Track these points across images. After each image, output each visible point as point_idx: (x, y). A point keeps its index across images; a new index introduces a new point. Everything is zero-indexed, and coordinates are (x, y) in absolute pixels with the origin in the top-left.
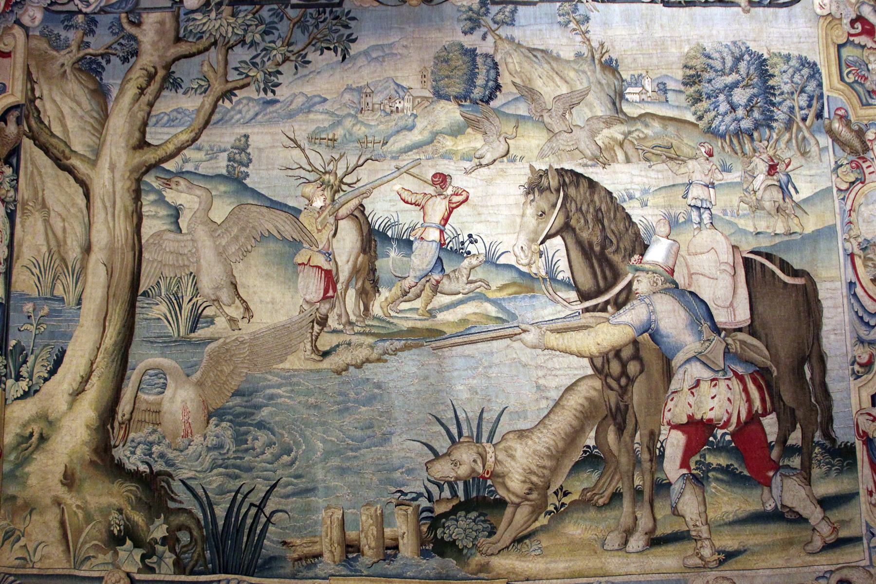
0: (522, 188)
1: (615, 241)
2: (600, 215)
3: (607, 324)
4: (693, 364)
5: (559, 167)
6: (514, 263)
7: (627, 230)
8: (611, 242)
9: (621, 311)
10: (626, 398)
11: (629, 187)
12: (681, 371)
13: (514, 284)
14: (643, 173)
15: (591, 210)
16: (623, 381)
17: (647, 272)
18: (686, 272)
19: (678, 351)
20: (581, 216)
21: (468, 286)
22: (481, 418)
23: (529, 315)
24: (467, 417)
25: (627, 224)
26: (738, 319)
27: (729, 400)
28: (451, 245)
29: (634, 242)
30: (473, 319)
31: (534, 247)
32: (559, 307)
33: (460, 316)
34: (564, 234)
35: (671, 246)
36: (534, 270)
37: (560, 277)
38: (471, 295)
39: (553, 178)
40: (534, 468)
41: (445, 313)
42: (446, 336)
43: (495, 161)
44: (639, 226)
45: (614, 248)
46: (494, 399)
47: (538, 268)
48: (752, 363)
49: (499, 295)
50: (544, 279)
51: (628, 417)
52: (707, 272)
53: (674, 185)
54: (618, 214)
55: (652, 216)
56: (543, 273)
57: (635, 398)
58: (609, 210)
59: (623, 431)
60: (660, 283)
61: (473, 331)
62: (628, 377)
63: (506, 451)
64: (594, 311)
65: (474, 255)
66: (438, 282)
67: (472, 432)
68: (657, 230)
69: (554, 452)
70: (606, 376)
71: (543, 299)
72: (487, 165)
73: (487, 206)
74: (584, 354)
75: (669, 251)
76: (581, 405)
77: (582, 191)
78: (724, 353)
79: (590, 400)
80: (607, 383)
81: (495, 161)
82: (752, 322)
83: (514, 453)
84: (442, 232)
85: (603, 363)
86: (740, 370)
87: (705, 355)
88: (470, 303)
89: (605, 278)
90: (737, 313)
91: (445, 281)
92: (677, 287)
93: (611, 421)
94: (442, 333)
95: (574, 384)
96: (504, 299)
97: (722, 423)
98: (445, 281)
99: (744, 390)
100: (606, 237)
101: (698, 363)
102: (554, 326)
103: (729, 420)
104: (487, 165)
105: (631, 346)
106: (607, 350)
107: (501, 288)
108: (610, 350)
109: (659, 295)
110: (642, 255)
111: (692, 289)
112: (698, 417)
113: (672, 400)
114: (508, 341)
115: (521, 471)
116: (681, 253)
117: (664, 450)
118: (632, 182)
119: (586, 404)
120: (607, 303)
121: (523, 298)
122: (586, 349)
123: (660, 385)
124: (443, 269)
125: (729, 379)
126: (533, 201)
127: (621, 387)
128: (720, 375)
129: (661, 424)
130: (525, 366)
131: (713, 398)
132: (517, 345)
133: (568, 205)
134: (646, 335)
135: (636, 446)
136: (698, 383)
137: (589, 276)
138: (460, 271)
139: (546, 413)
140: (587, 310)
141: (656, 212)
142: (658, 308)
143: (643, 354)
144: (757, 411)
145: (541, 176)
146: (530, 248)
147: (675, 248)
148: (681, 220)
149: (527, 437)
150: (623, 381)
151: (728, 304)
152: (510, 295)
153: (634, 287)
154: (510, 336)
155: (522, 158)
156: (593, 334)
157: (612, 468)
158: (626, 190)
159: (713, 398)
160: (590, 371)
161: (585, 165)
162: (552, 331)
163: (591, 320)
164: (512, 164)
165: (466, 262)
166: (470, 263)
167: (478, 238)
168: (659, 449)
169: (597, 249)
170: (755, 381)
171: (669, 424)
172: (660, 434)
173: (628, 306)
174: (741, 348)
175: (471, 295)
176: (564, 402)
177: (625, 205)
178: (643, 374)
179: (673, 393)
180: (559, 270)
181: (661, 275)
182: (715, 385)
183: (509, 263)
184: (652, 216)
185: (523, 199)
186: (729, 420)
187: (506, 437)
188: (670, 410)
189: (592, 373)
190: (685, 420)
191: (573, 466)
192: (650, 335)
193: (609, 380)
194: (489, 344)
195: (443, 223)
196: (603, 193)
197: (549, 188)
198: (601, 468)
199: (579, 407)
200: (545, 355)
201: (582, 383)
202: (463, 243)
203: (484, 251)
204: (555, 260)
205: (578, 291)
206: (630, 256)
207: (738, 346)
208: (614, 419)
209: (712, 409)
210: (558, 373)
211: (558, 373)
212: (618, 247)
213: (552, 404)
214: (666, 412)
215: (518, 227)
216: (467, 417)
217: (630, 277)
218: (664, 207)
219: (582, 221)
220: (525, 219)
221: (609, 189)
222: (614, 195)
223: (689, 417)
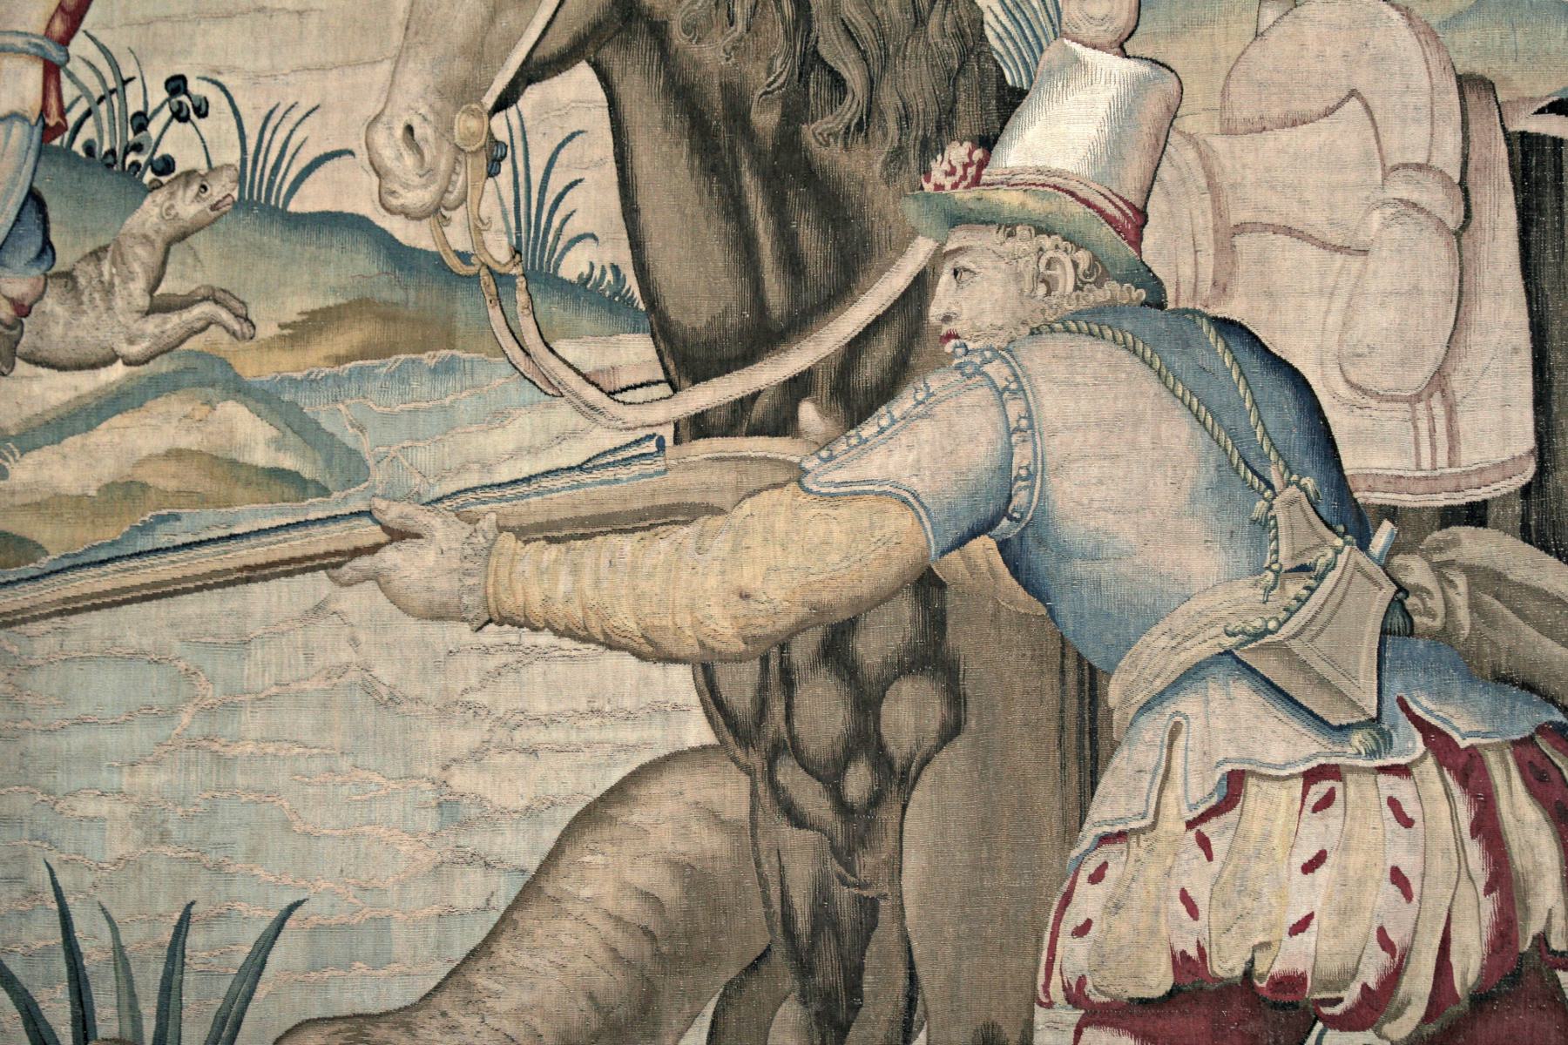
1: (854, 76)
3: (787, 495)
4: (1215, 691)
6: (365, 206)
7: (920, 21)
8: (838, 83)
9: (868, 430)
10: (866, 862)
12: (1153, 729)
13: (359, 307)
16: (858, 783)
17: (1009, 227)
18: (1204, 220)
19: (1144, 629)
21: (152, 325)
22: (176, 951)
23: (424, 456)
24: (119, 949)
26: (1469, 457)
27: (1398, 877)
28: (88, 131)
29: (952, 78)
30: (165, 479)
32: (563, 415)
33: (108, 469)
34: (608, 54)
35: (1139, 87)
36: (458, 238)
37: (573, 266)
38: (162, 366)
41: (47, 454)
42: (44, 563)
45: (849, 110)
46: (238, 866)
47: (477, 227)
48: (1529, 687)
49: (287, 363)
50: (502, 280)
51: (871, 960)
52: (1316, 219)
56: (499, 250)
57: (913, 863)
60: (1066, 281)
61: (162, 540)
62: (881, 760)
64: (729, 430)
65: (189, 175)
66: (22, 309)
67: (136, 1019)
70: (775, 753)
71: (498, 378)
74: (669, 645)
75: (1124, 113)
76: (646, 896)
78: (1384, 632)
79: (690, 874)
80: (774, 786)
82: (1541, 471)
84: (52, 71)
85: (763, 687)
86: (1464, 726)
87: (1282, 649)
88: (158, 406)
89: (792, 262)
90: (1464, 422)
91: (53, 304)
92: (1156, 300)
94: (24, 547)
95: (619, 793)
96: (311, 382)
97: (1351, 995)
98: (53, 304)
99: (1476, 830)
100: (810, 60)
101: (1242, 691)
102: (535, 508)
103: (1392, 979)
105: (906, 608)
106: (785, 622)
107: (301, 331)
108: (800, 627)
110: (988, 143)
111: (1233, 310)
112: (1227, 964)
113: (1096, 878)
114: (316, 585)
116: (1187, 123)
119: (670, 892)
120: (799, 386)
121: (400, 377)
122: (684, 620)
123: (1048, 800)
124: (47, 247)
125: (1402, 771)
127: (843, 807)
128: (1353, 751)
129: (1035, 1000)
130: (390, 702)
131: (1309, 868)
132: (358, 601)
134: (983, 548)
136: (1234, 786)
137: (718, 255)
138: (120, 260)
139: (479, 935)
140: (699, 426)
142: (1052, 404)
143: (959, 640)
144: (1542, 940)
147: (1153, 107)
150: (858, 783)
151: (1419, 376)
152: (339, 360)
153: (935, 311)
154: (329, 562)
156: (721, 546)
159: (1309, 868)
160: (697, 731)
162: (525, 534)
163: (712, 476)
165: (150, 213)
166: (168, 214)
167: (213, 95)
169: (766, 120)
170: (1538, 779)
171: (1075, 996)
173: (904, 403)
174: (1475, 606)
175: (162, 366)
176: (562, 883)
178: (960, 743)
179: (1105, 839)
180: (571, 230)
181: (1075, 241)
182: (1327, 801)
183: (347, 207)
186: (1392, 979)
188: (1082, 930)
189: (706, 736)
190: (1158, 980)
192: (1003, 546)
193: (789, 774)
194: (234, 598)
195: (59, 27)
199: (631, 908)
200: (486, 651)
201: (654, 788)
202: (141, 121)
203: (234, 157)
204: (556, 185)
205: (663, 332)
206: (929, 149)
207: (1461, 601)
208: (804, 969)
209: (1301, 926)
210: (538, 736)
211: (538, 736)
212: (871, 108)
213: (506, 889)
214: (1065, 942)
215: (397, 36)
216: (119, 949)
217: (919, 253)
223: (1181, 963)
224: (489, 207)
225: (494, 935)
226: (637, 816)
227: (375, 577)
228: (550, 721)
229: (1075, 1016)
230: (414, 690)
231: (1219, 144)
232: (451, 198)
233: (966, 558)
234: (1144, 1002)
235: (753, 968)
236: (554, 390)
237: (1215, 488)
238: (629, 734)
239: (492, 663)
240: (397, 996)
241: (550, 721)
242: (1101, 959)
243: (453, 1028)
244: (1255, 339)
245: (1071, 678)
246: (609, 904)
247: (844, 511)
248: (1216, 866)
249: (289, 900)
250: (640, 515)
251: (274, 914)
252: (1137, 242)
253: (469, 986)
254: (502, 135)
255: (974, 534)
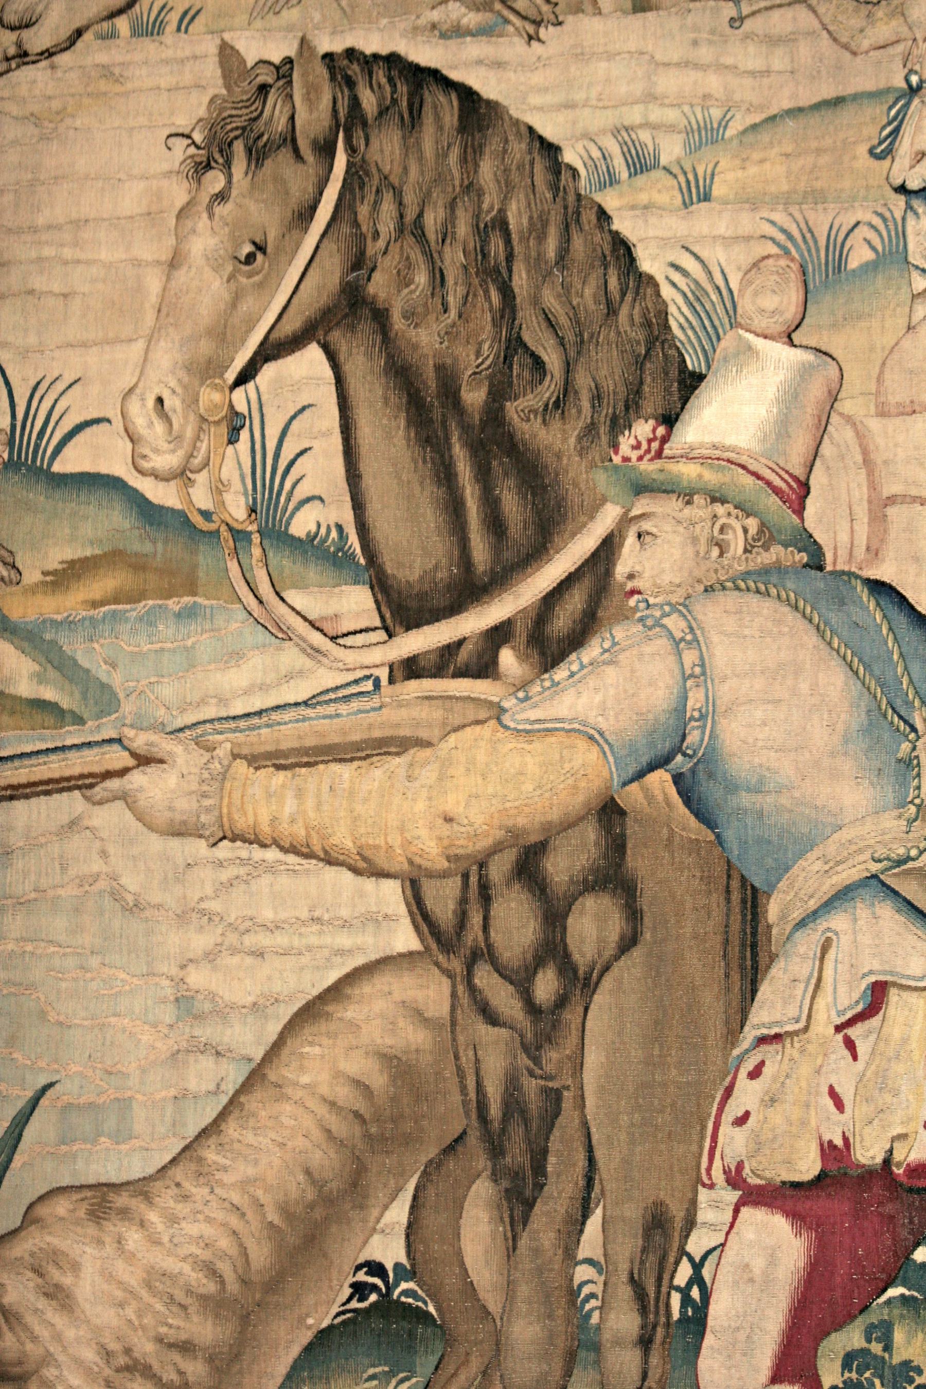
0: (180, 144)
1: (552, 359)
2: (496, 246)
4: (862, 911)
5: (337, 46)
6: (120, 469)
7: (612, 311)
8: (538, 364)
9: (560, 674)
10: (552, 1057)
11: (634, 115)
14: (705, 54)
15: (463, 228)
17: (687, 496)
18: (860, 493)
19: (801, 855)
20: (416, 255)
23: (167, 691)
25: (613, 283)
29: (640, 363)
31: (210, 397)
32: (291, 657)
34: (336, 336)
35: (804, 373)
36: (201, 498)
39: (312, 92)
40: (146, 1348)
43: (79, 33)
44: (667, 292)
45: (548, 390)
47: (218, 488)
50: (239, 536)
51: (554, 1144)
53: (838, 102)
54: (578, 243)
55: (729, 241)
57: (593, 1058)
58: (538, 229)
59: (530, 1205)
60: (737, 544)
62: (567, 967)
63: (38, 1272)
68: (746, 305)
69: (233, 1286)
70: (473, 958)
72: (48, 54)
73: (34, 229)
74: (382, 862)
76: (357, 1083)
77: (428, 146)
80: (472, 989)
81: (79, 33)
83: (67, 1280)
85: (463, 901)
92: (817, 564)
93: (482, 1162)
96: (69, 624)
101: (887, 911)
104: (48, 54)
105: (591, 833)
106: (484, 843)
108: (497, 849)
109: (730, 599)
110: (670, 420)
111: (884, 572)
113: (755, 1074)
114: (73, 803)
115: (89, 1355)
116: (846, 406)
117: (706, 1295)
118: (650, 97)
119: (379, 1080)
121: (149, 620)
122: (395, 840)
126: (221, 197)
127: (532, 1008)
130: (136, 907)
133: (363, 211)
134: (660, 779)
135: (583, 1273)
141: (748, 223)
145: (263, 89)
146: (192, 401)
147: (816, 391)
148: (859, 256)
149: (124, 1213)
152: (95, 604)
153: (621, 570)
155: (188, 18)
156: (428, 775)
157: (475, 1364)
158: (621, 131)
161: (457, 32)
162: (255, 761)
163: (423, 712)
164: (148, 47)
168: (685, 1292)
171: (735, 1179)
172: (690, 1224)
173: (592, 651)
177: (610, 201)
178: (637, 953)
179: (763, 1040)
183: (104, 470)
184: (729, 241)
185: (179, 193)
187: (42, 1211)
188: (742, 1120)
189: (415, 944)
191: (309, 1349)
192: (678, 779)
193: (485, 977)
196: (518, 148)
197: (290, 139)
198: (425, 1364)
199: (344, 1094)
201: (366, 988)
206: (617, 425)
208: (496, 1150)
210: (263, 940)
211: (263, 940)
212: (568, 388)
213: (235, 1076)
214: (726, 1129)
215: (150, 317)
218: (786, 200)
219: (421, 278)
220: (182, 276)
221: (548, 130)
222: (569, 156)
223: (828, 1151)
224: (229, 471)
225: (223, 1115)
226: (351, 1012)
227: (124, 797)
228: (276, 927)
229: (733, 1196)
230: (156, 897)
231: (874, 424)
232: (196, 462)
233: (646, 791)
234: (796, 1185)
235: (451, 1149)
236: (283, 634)
237: (867, 730)
238: (344, 940)
239: (225, 875)
240: (137, 1168)
241: (276, 927)
242: (757, 1146)
243: (186, 1198)
244: (903, 599)
245: (736, 896)
246: (324, 1090)
247: (537, 746)
248: (860, 1065)
249: (42, 1081)
250: (357, 746)
251: (30, 1094)
252: (800, 510)
253: (200, 1160)
254: (242, 407)
255: (651, 768)
